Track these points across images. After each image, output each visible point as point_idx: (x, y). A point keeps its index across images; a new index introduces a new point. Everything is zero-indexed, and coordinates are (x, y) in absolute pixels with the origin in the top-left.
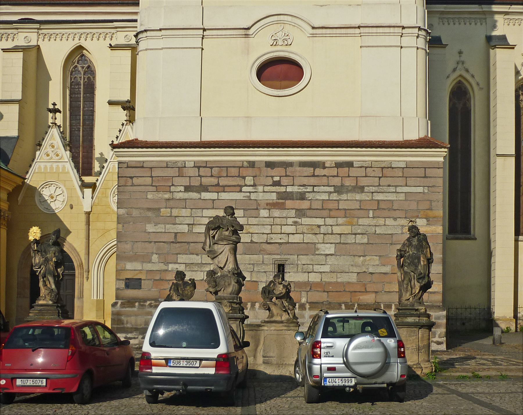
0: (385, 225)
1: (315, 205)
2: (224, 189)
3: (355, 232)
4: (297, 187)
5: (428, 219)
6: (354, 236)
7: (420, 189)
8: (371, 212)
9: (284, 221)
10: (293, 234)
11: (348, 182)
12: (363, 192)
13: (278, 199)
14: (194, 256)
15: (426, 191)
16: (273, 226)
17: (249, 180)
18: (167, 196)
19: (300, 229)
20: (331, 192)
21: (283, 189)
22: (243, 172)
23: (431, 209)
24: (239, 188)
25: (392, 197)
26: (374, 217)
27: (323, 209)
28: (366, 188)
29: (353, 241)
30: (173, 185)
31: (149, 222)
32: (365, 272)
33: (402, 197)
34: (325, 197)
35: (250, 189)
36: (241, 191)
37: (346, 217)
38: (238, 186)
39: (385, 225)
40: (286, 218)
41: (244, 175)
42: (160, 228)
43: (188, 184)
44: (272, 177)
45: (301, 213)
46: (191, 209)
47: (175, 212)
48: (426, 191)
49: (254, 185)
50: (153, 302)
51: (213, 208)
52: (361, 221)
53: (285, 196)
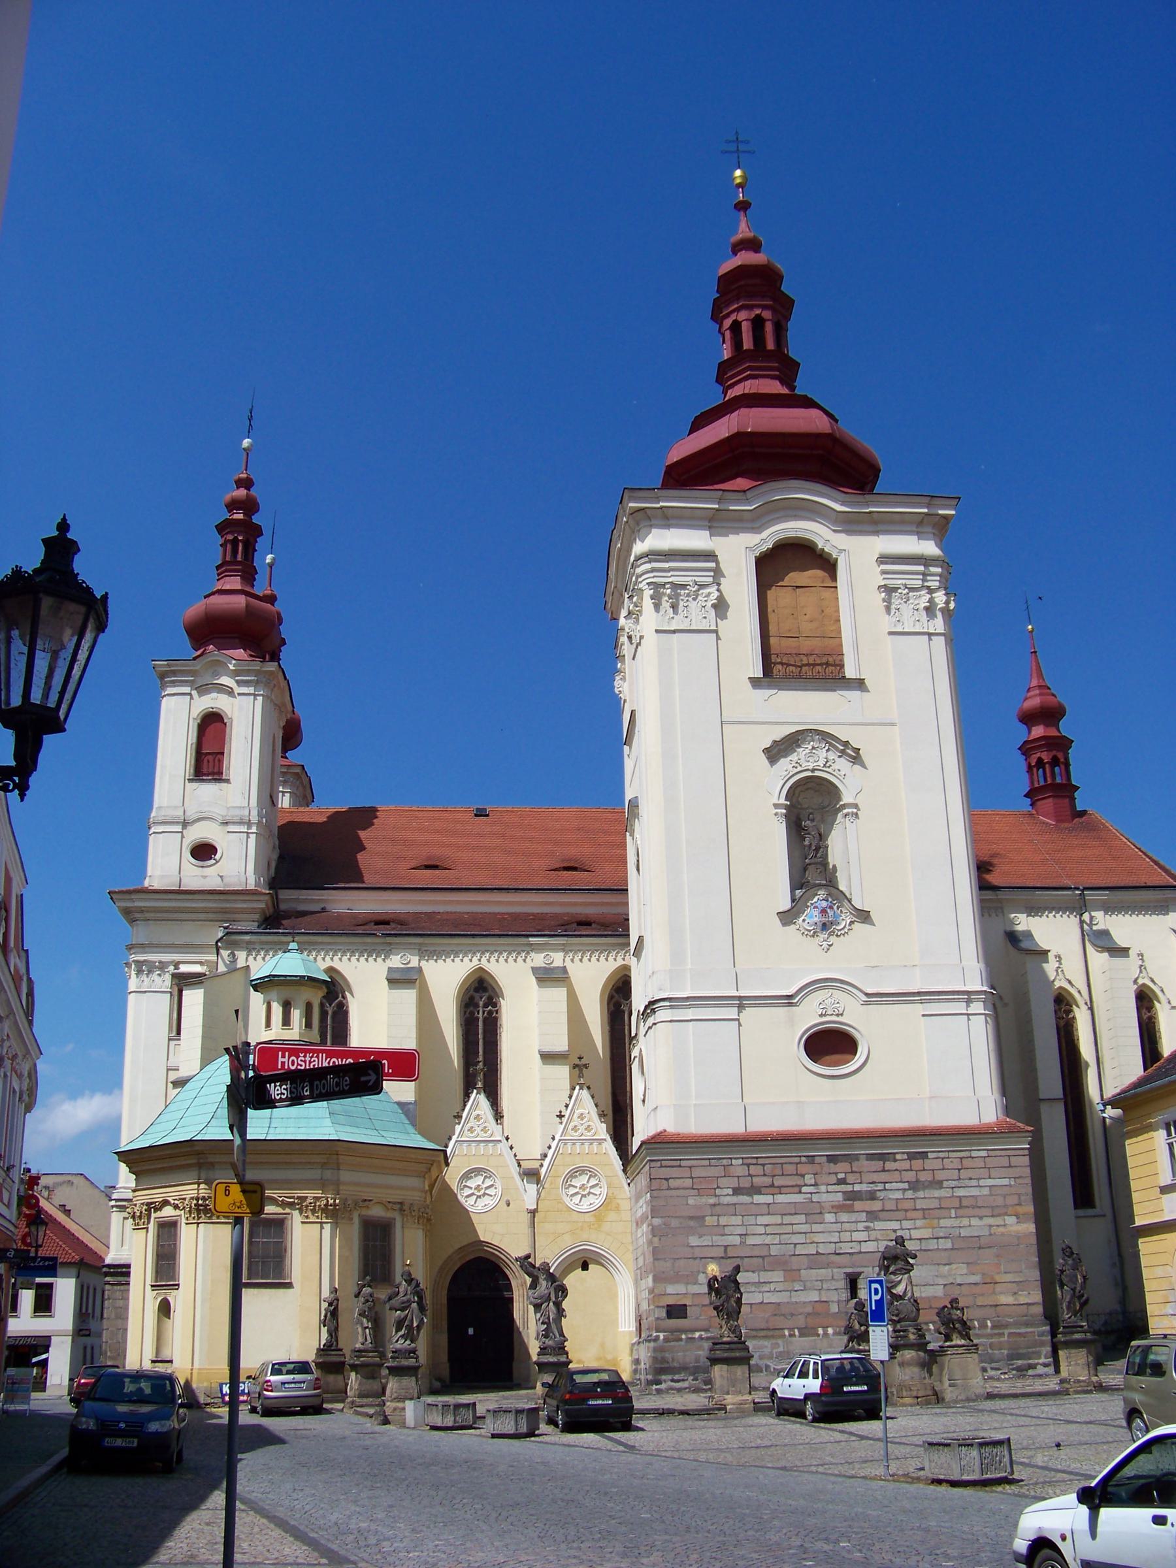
0: (970, 1226)
1: (890, 1205)
2: (780, 1190)
3: (938, 1236)
4: (865, 1185)
5: (1017, 1216)
6: (936, 1240)
7: (1005, 1182)
8: (953, 1211)
9: (853, 1227)
10: (866, 1241)
11: (925, 1177)
12: (941, 1187)
13: (845, 1200)
14: (750, 1274)
15: (1013, 1183)
16: (842, 1233)
17: (809, 1179)
18: (712, 1201)
19: (873, 1234)
20: (905, 1190)
21: (849, 1188)
22: (802, 1169)
23: (1019, 1204)
24: (798, 1189)
25: (975, 1192)
26: (956, 1217)
27: (897, 1210)
28: (945, 1183)
29: (936, 1247)
30: (718, 1187)
31: (693, 1234)
32: (952, 1283)
33: (986, 1191)
34: (899, 1195)
35: (811, 1189)
36: (800, 1192)
37: (924, 1218)
38: (797, 1186)
39: (970, 1226)
40: (857, 1222)
41: (803, 1173)
42: (706, 1241)
43: (737, 1186)
44: (836, 1174)
45: (872, 1216)
46: (743, 1216)
47: (723, 1220)
48: (1013, 1183)
49: (816, 1185)
50: (703, 1333)
51: (769, 1214)
52: (943, 1222)
53: (853, 1196)
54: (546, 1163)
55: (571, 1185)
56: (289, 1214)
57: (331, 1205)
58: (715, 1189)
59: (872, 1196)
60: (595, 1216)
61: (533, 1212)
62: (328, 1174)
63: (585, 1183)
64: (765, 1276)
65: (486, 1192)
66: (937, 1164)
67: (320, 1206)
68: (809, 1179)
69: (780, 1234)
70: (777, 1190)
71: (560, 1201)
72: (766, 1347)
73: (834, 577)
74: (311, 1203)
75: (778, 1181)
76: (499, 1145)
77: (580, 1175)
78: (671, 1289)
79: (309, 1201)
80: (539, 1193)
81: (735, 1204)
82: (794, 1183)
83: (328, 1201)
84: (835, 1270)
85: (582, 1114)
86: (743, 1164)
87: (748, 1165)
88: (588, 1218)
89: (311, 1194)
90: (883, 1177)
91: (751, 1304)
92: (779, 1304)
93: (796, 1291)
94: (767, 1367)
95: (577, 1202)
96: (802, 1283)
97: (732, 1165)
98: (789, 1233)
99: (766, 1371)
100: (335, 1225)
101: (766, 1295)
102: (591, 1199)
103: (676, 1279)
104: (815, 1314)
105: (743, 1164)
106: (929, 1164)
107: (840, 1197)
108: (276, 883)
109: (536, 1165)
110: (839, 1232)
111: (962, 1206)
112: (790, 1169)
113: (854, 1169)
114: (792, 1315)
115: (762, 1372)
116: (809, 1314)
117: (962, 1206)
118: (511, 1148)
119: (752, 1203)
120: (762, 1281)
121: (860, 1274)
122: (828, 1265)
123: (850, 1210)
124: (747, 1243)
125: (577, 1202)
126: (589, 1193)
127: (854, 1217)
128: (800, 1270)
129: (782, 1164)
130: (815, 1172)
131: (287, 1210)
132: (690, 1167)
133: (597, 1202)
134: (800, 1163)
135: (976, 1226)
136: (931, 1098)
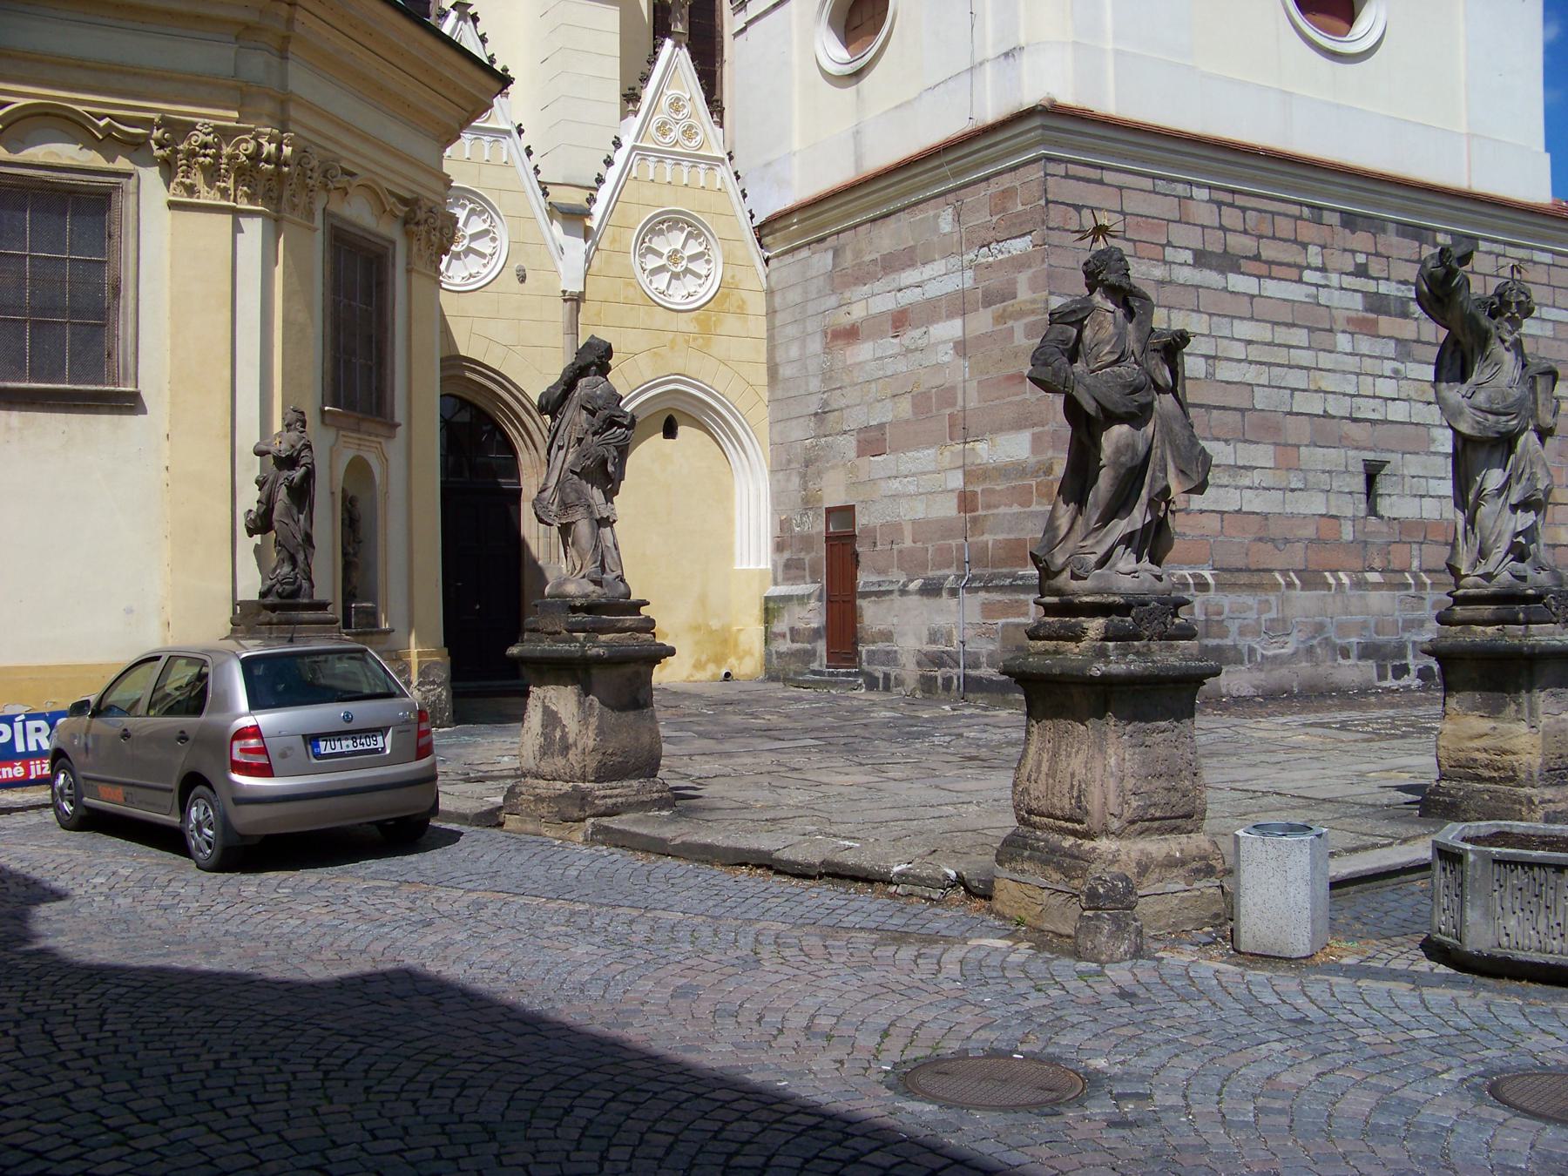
13: (1366, 310)
17: (1314, 256)
19: (1408, 389)
21: (1371, 286)
30: (1169, 244)
36: (1300, 281)
41: (1306, 240)
44: (1354, 252)
51: (1252, 318)
54: (604, 194)
55: (651, 250)
56: (129, 175)
57: (267, 161)
58: (1163, 246)
60: (697, 319)
61: (576, 300)
62: (257, 65)
63: (679, 247)
65: (473, 245)
67: (235, 157)
68: (1314, 256)
69: (1269, 365)
70: (1264, 269)
71: (630, 280)
72: (1251, 608)
74: (205, 146)
75: (1269, 251)
76: (506, 143)
77: (670, 229)
79: (198, 138)
80: (588, 260)
81: (1197, 287)
82: (1290, 260)
83: (260, 145)
84: (1351, 453)
85: (678, 99)
86: (1211, 201)
87: (1220, 204)
88: (684, 323)
89: (206, 117)
91: (1222, 513)
92: (1266, 516)
93: (1293, 490)
94: (1252, 651)
95: (663, 287)
96: (1301, 475)
97: (1191, 198)
98: (1282, 366)
99: (1250, 662)
100: (275, 225)
101: (1248, 494)
102: (690, 283)
104: (1317, 542)
105: (1211, 201)
107: (1357, 302)
109: (577, 198)
110: (1358, 374)
112: (1284, 227)
113: (1381, 249)
114: (1287, 541)
115: (1242, 663)
116: (1311, 541)
118: (529, 152)
119: (1225, 289)
120: (1240, 463)
121: (1383, 464)
122: (1341, 442)
124: (1218, 377)
125: (663, 287)
126: (687, 271)
128: (1298, 446)
129: (1273, 213)
130: (1322, 243)
131: (122, 164)
132: (1120, 188)
133: (706, 291)
134: (1300, 218)
136: (1470, 136)
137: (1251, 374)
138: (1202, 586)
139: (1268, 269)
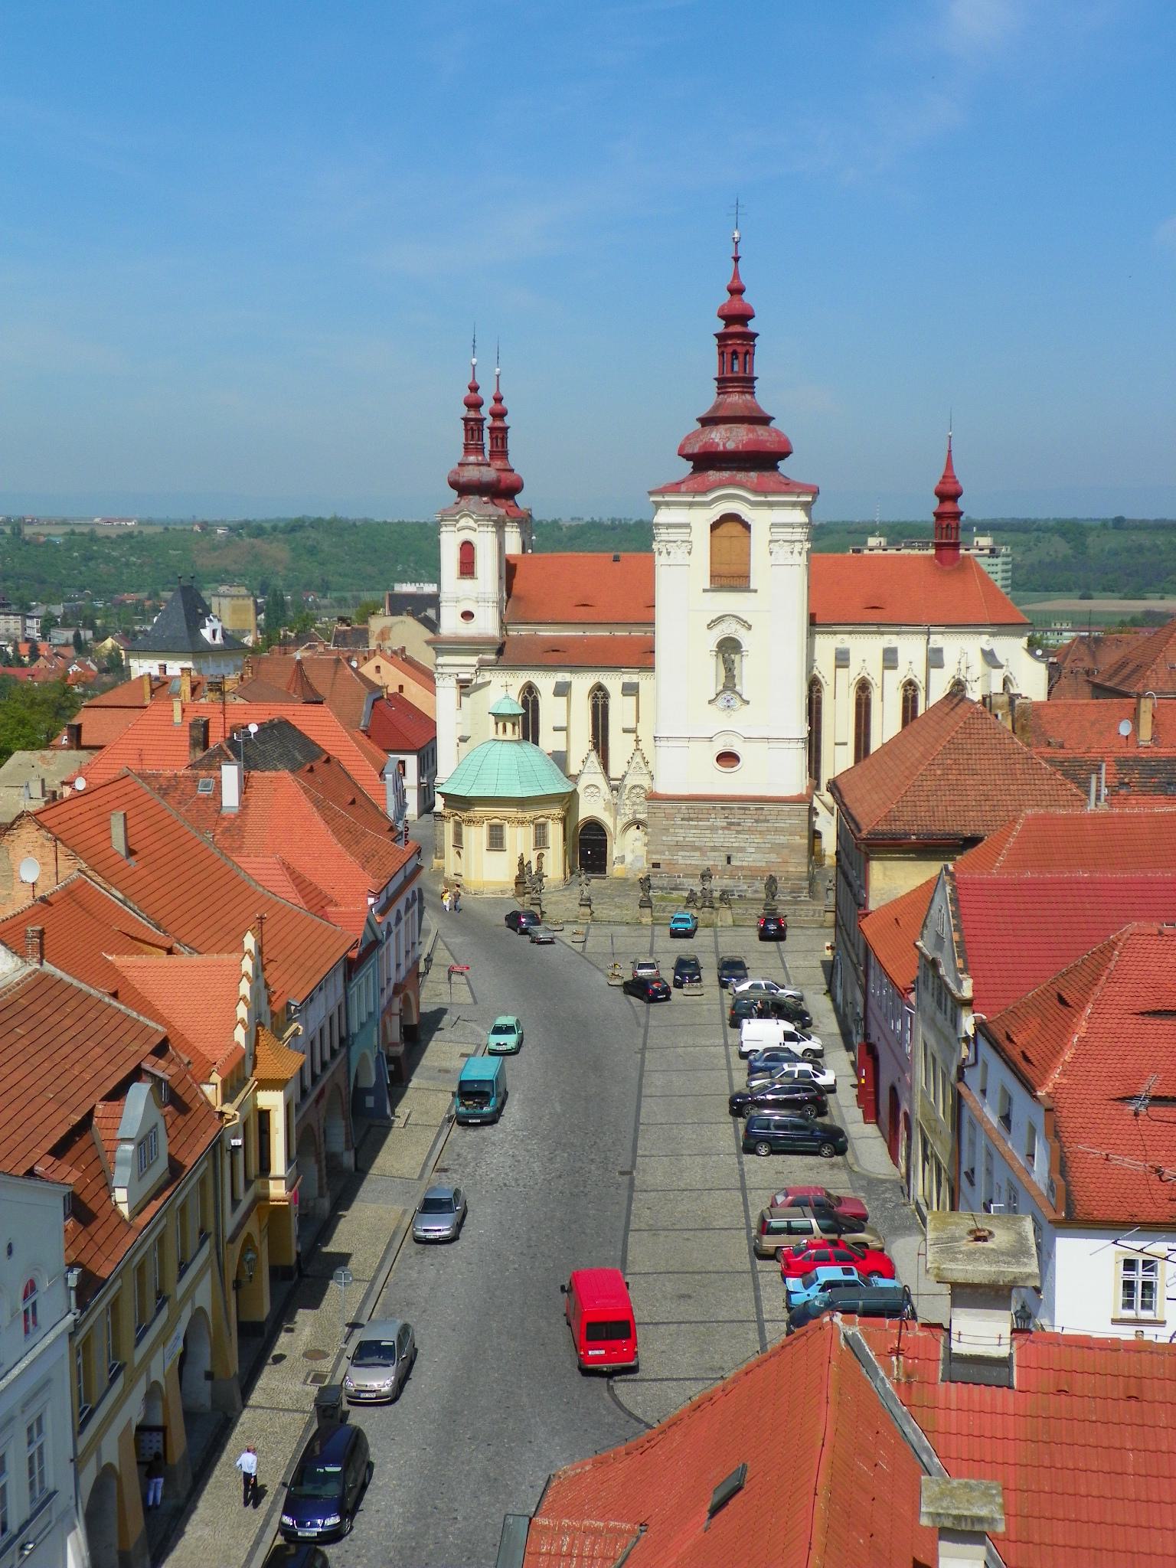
2: (701, 820)
11: (761, 817)
17: (713, 816)
22: (710, 812)
25: (783, 825)
45: (738, 832)
47: (677, 831)
52: (768, 837)
59: (739, 824)
64: (692, 854)
66: (768, 813)
68: (713, 816)
73: (750, 532)
78: (654, 857)
90: (744, 816)
103: (656, 853)
106: (764, 813)
108: (503, 625)
111: (777, 831)
117: (777, 831)
123: (729, 829)
127: (730, 832)
135: (782, 839)
137: (694, 839)
138: (679, 877)
139: (699, 820)
